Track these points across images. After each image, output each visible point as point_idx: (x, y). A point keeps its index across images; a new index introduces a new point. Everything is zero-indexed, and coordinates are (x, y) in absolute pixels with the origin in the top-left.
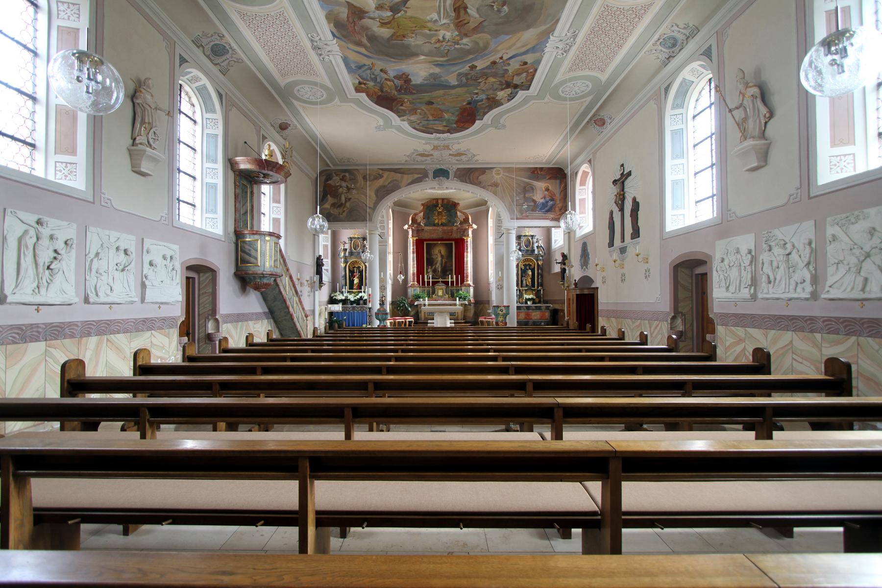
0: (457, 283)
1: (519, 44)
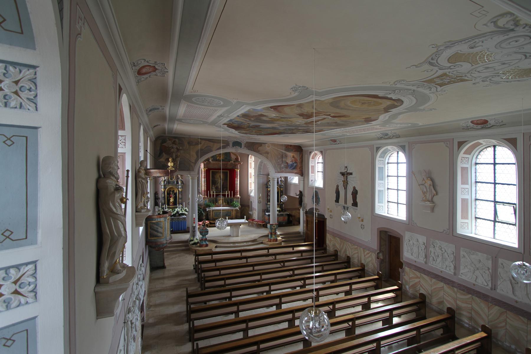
0: (231, 195)
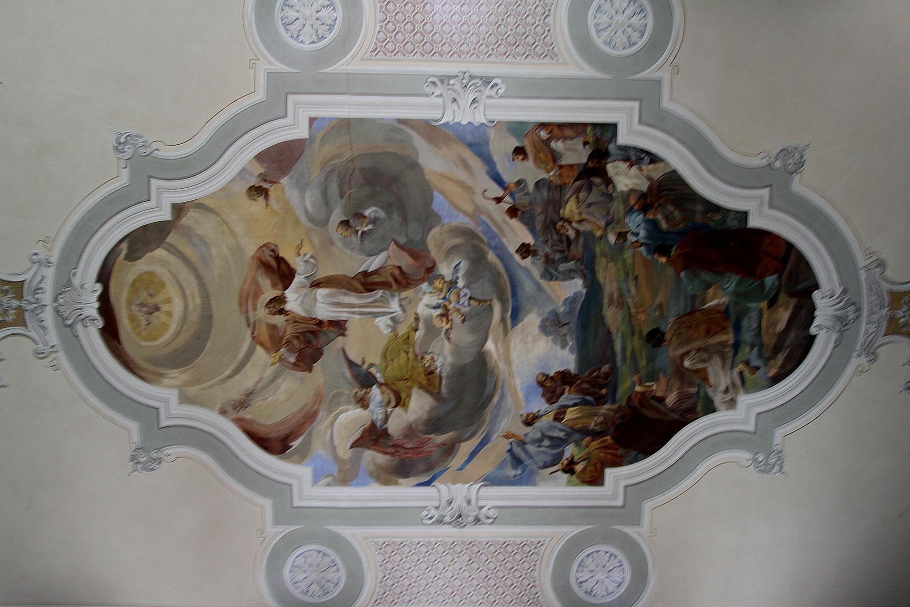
1: (461, 174)
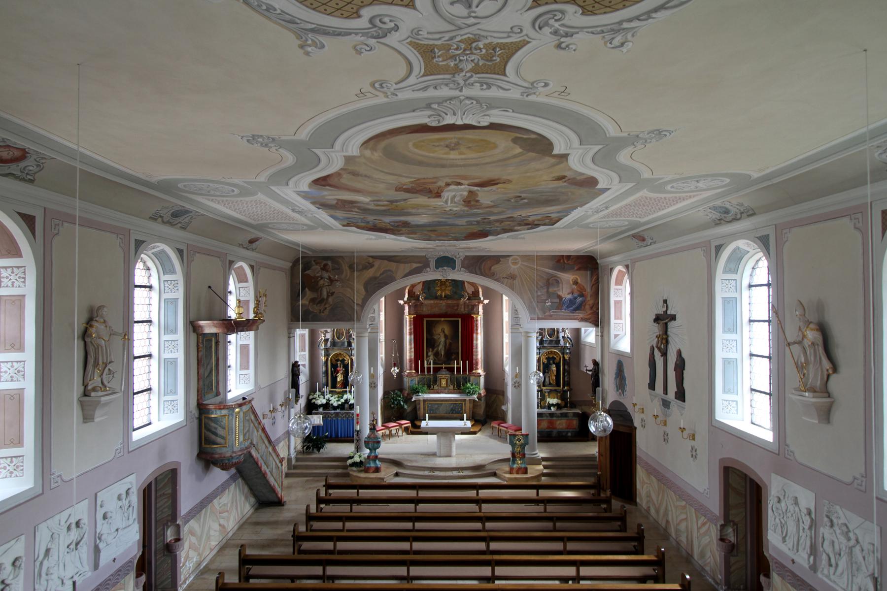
0: (464, 370)
